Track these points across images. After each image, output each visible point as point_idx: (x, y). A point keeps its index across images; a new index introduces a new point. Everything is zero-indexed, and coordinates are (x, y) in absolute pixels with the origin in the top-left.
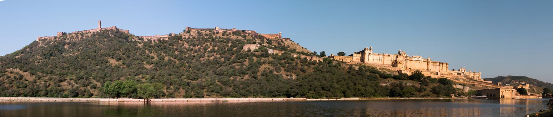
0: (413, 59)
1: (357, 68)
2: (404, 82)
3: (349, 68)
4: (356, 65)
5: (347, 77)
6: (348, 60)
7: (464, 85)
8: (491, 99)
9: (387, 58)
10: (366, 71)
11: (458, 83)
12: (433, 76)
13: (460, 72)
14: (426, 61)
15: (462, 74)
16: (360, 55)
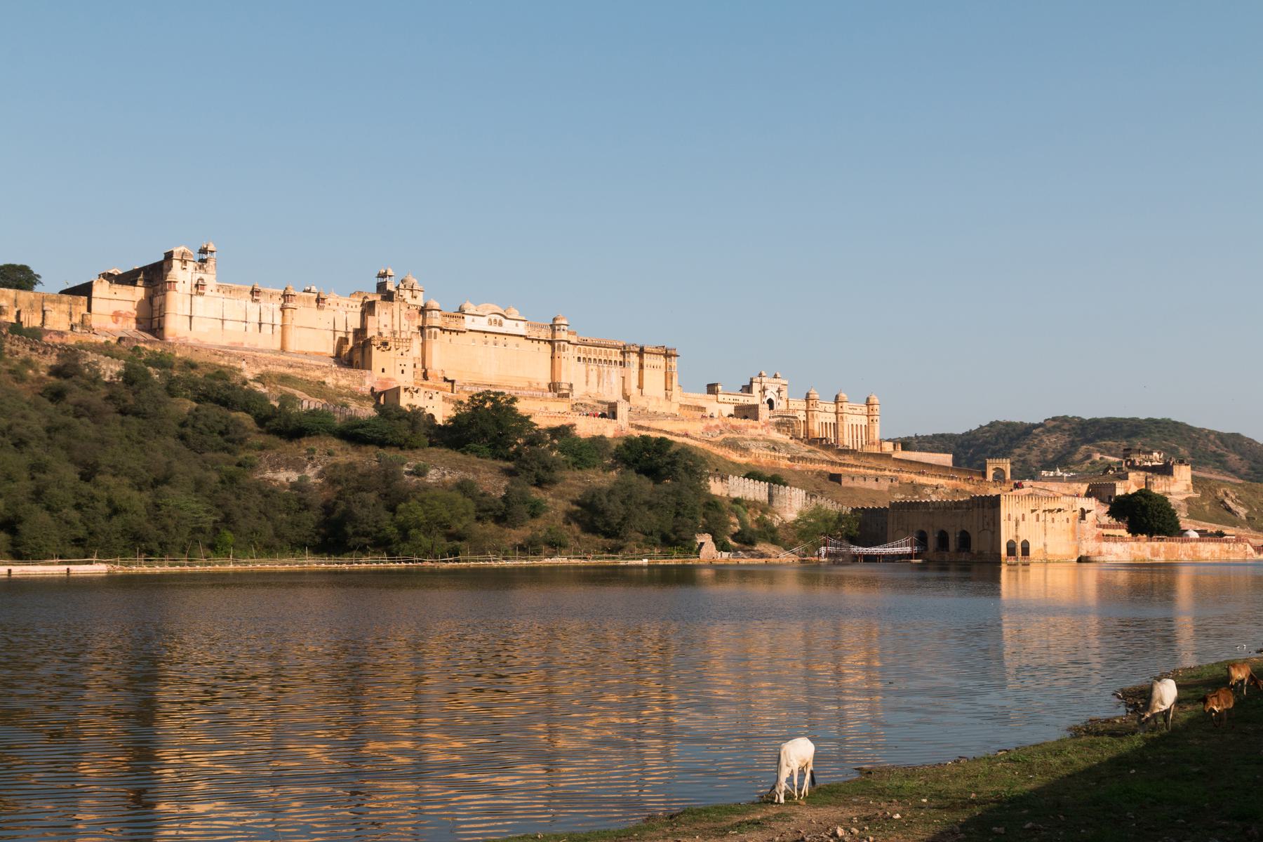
0: (468, 323)
1: (111, 369)
2: (410, 461)
3: (55, 372)
4: (106, 350)
5: (36, 422)
6: (58, 319)
7: (775, 480)
8: (943, 567)
9: (304, 313)
10: (171, 391)
11: (737, 469)
12: (586, 427)
13: (755, 399)
15: (764, 412)
16: (139, 292)
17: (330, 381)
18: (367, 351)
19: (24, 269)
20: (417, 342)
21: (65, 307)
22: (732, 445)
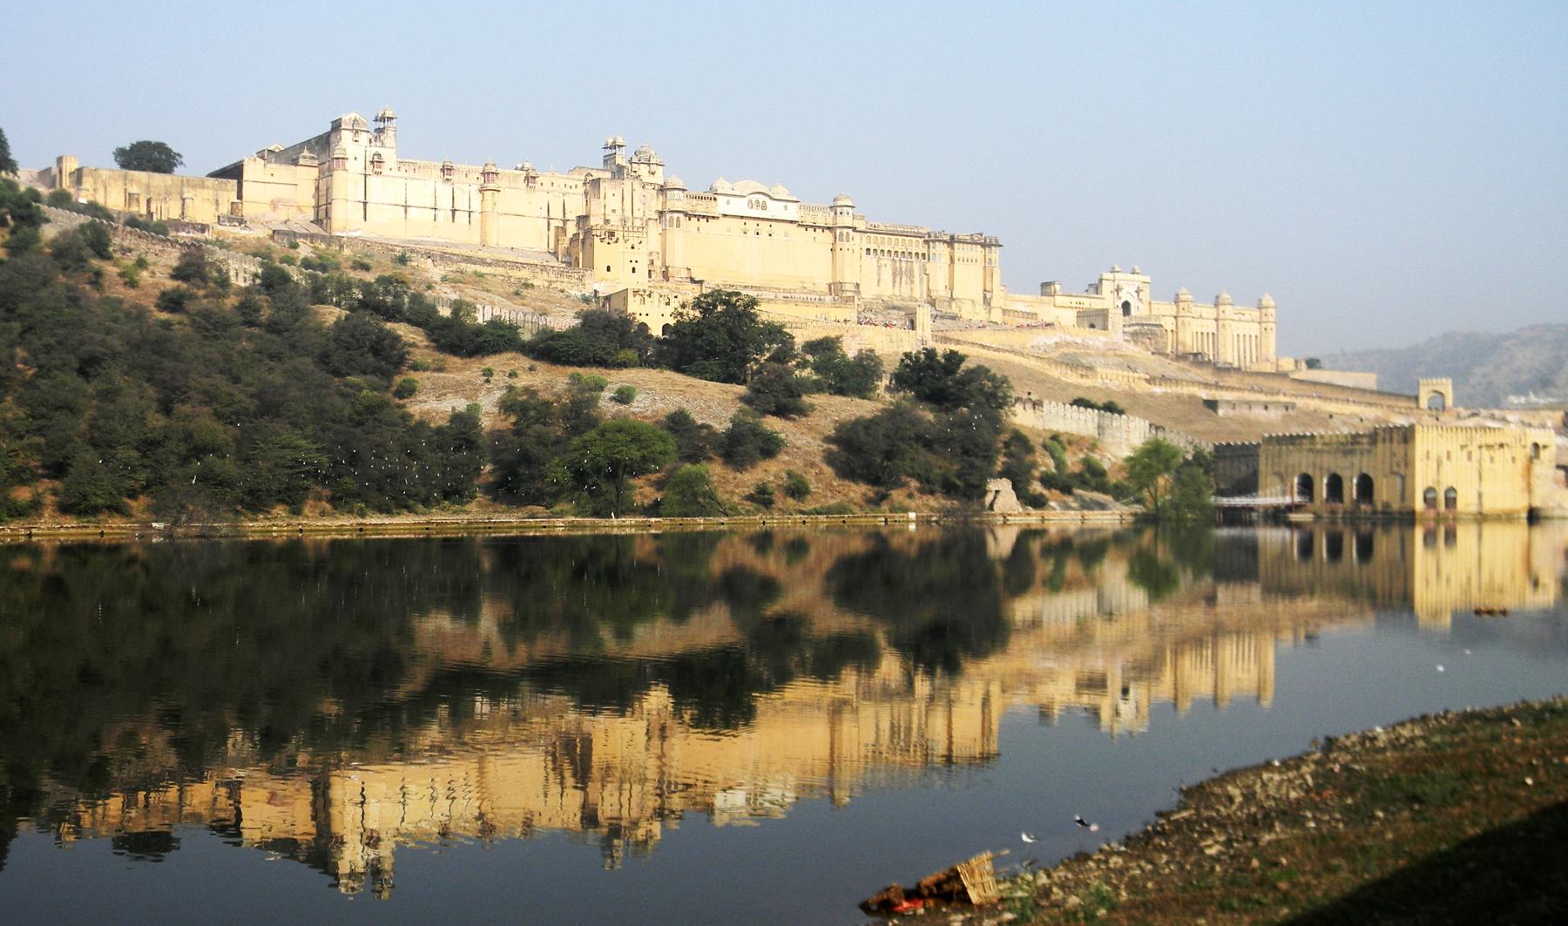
0: (721, 206)
9: (512, 195)
18: (588, 242)
19: (161, 147)
21: (208, 194)
22: (1072, 363)
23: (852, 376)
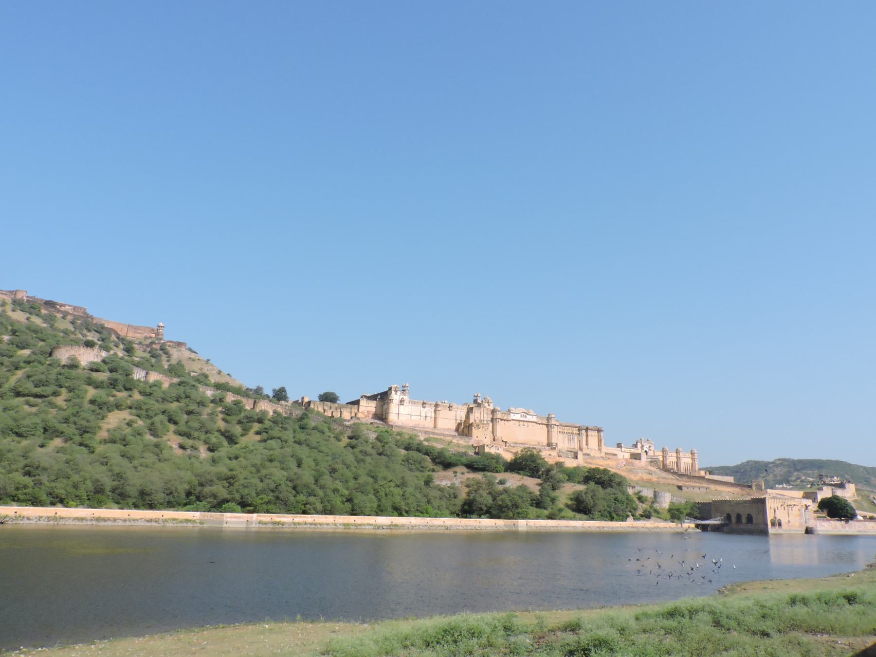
0: (512, 416)
2: (499, 476)
12: (570, 463)
14: (545, 422)
17: (454, 441)
20: (491, 424)
23: (571, 475)
